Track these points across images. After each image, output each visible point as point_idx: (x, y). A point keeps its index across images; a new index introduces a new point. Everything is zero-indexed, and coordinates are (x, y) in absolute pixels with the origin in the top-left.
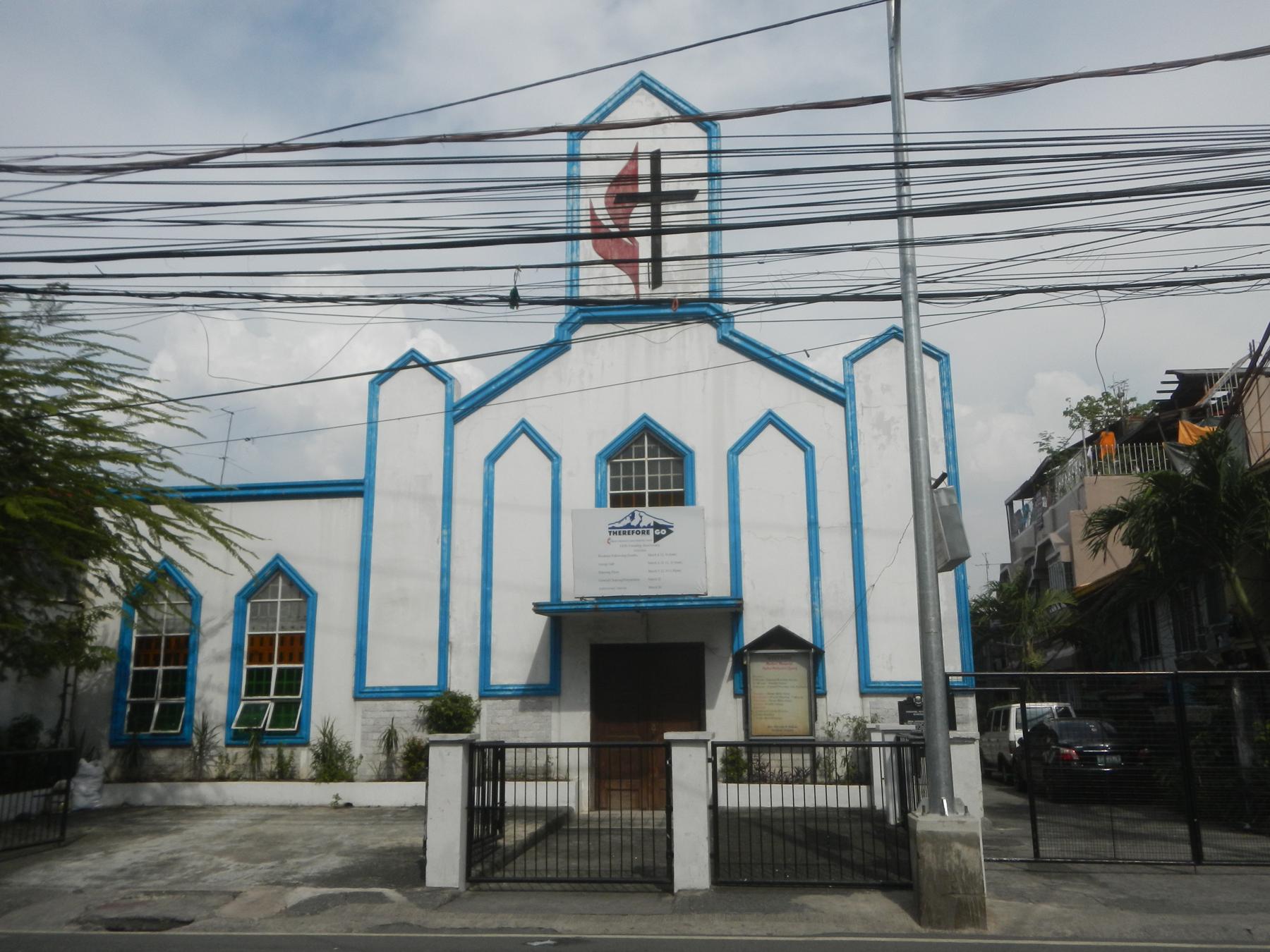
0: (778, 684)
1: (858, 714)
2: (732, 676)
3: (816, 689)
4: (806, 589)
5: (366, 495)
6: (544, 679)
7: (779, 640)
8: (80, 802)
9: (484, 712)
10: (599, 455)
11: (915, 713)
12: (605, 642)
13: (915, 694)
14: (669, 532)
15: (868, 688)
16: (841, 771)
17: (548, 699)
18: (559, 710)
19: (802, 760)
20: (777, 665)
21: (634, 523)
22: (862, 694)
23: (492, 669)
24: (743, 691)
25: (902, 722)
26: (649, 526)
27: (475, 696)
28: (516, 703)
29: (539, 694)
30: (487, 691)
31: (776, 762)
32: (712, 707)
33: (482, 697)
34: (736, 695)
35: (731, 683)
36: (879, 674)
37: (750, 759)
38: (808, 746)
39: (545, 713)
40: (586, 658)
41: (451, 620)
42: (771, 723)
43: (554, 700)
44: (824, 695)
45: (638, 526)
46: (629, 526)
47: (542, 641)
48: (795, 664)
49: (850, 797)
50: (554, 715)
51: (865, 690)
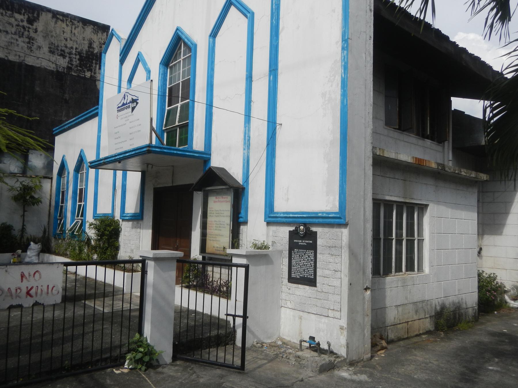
5: (99, 114)
8: (27, 260)
10: (160, 64)
11: (300, 242)
12: (158, 186)
14: (137, 103)
21: (125, 103)
22: (269, 224)
26: (130, 102)
28: (131, 223)
29: (137, 218)
32: (195, 231)
33: (123, 220)
39: (139, 230)
44: (245, 223)
45: (126, 104)
46: (124, 104)
50: (141, 230)
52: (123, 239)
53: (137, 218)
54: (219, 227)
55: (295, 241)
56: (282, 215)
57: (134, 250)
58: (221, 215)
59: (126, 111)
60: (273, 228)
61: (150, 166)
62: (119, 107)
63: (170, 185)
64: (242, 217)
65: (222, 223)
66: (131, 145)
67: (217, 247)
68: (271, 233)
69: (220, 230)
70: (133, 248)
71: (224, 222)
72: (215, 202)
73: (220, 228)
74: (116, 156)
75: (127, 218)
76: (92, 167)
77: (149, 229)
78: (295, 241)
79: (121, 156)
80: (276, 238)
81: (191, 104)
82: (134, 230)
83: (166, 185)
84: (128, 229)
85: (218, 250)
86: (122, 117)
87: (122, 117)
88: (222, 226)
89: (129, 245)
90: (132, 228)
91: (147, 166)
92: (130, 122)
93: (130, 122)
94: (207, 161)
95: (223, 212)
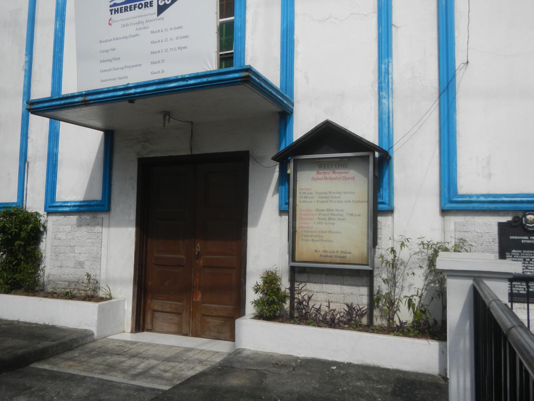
0: (332, 198)
1: (436, 238)
2: (277, 190)
3: (379, 206)
4: (372, 77)
6: (97, 195)
7: (331, 142)
9: (49, 226)
11: (525, 239)
12: (151, 156)
13: (526, 212)
15: (453, 204)
16: (405, 315)
17: (101, 216)
18: (109, 226)
19: (358, 296)
20: (330, 174)
22: (444, 212)
23: (58, 186)
24: (289, 209)
25: (502, 256)
27: (42, 212)
28: (73, 219)
29: (93, 210)
30: (53, 208)
31: (325, 295)
33: (49, 213)
34: (282, 212)
35: (277, 197)
36: (471, 182)
37: (292, 289)
38: (363, 275)
39: (98, 229)
40: (133, 172)
41: (29, 140)
42: (320, 246)
43: (105, 216)
44: (390, 212)
47: (97, 158)
48: (352, 173)
49: (416, 356)
50: (105, 230)
51: (449, 206)
52: (47, 246)
53: (93, 210)
54: (329, 219)
55: (511, 237)
56: (482, 199)
57: (87, 263)
58: (337, 199)
59: (144, 11)
60: (453, 220)
61: (167, 117)
62: (115, 5)
63: (189, 153)
64: (382, 203)
65: (335, 213)
66: (153, 73)
67: (326, 251)
68: (452, 227)
69: (333, 224)
70: (81, 259)
71: (342, 210)
72: (313, 179)
73: (331, 221)
74: (115, 90)
75: (67, 209)
76: (35, 112)
77: (127, 225)
78: (511, 237)
79: (139, 90)
80: (466, 234)
81: (237, 25)
82: (84, 229)
83: (174, 154)
84: (68, 228)
85: (327, 256)
86: (129, 22)
87: (129, 22)
88: (336, 217)
89: (72, 255)
90: (79, 225)
91: (165, 116)
92: (152, 32)
93: (152, 32)
94: (285, 115)
95: (338, 195)
